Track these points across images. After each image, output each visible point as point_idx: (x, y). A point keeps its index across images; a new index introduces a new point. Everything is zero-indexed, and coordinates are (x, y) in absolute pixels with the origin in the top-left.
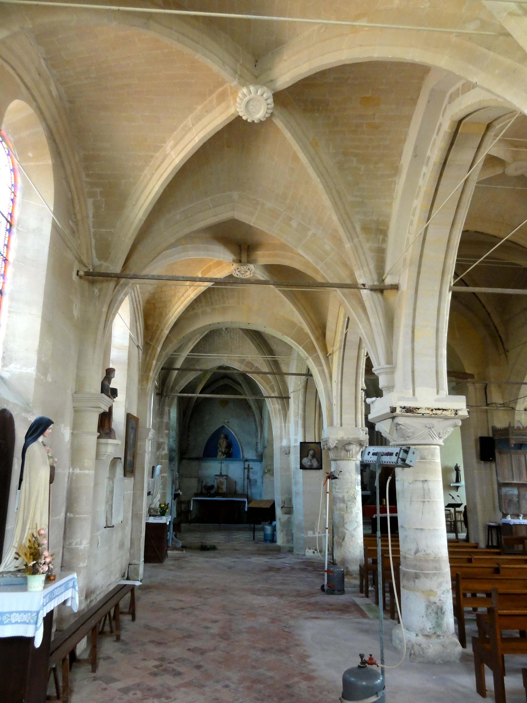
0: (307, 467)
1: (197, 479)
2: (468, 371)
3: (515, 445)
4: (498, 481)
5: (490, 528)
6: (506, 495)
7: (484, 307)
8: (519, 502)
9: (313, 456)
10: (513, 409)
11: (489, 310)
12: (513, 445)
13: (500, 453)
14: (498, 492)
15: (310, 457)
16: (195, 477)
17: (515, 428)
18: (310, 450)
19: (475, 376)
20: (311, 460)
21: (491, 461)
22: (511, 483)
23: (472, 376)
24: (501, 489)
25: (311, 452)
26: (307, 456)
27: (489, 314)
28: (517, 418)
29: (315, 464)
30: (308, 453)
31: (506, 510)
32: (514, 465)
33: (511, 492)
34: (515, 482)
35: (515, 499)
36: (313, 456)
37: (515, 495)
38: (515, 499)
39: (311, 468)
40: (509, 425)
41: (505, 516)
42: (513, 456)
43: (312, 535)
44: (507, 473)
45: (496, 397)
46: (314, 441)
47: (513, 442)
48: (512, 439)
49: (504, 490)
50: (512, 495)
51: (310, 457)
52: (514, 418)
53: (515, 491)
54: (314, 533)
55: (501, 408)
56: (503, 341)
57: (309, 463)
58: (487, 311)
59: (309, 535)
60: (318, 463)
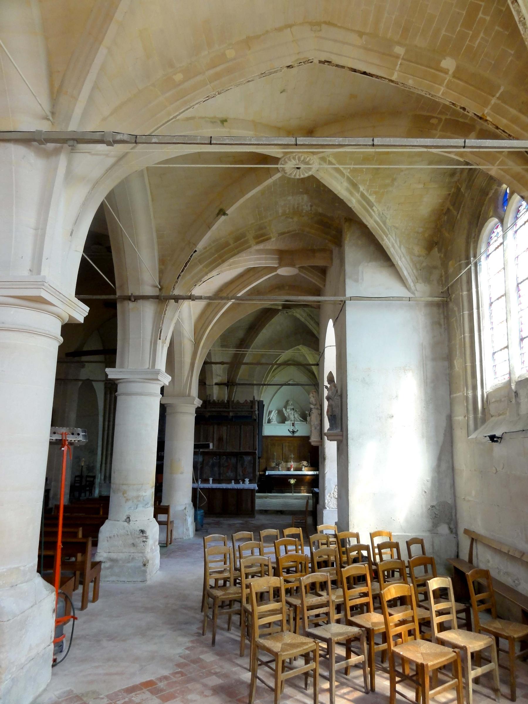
10: (205, 384)
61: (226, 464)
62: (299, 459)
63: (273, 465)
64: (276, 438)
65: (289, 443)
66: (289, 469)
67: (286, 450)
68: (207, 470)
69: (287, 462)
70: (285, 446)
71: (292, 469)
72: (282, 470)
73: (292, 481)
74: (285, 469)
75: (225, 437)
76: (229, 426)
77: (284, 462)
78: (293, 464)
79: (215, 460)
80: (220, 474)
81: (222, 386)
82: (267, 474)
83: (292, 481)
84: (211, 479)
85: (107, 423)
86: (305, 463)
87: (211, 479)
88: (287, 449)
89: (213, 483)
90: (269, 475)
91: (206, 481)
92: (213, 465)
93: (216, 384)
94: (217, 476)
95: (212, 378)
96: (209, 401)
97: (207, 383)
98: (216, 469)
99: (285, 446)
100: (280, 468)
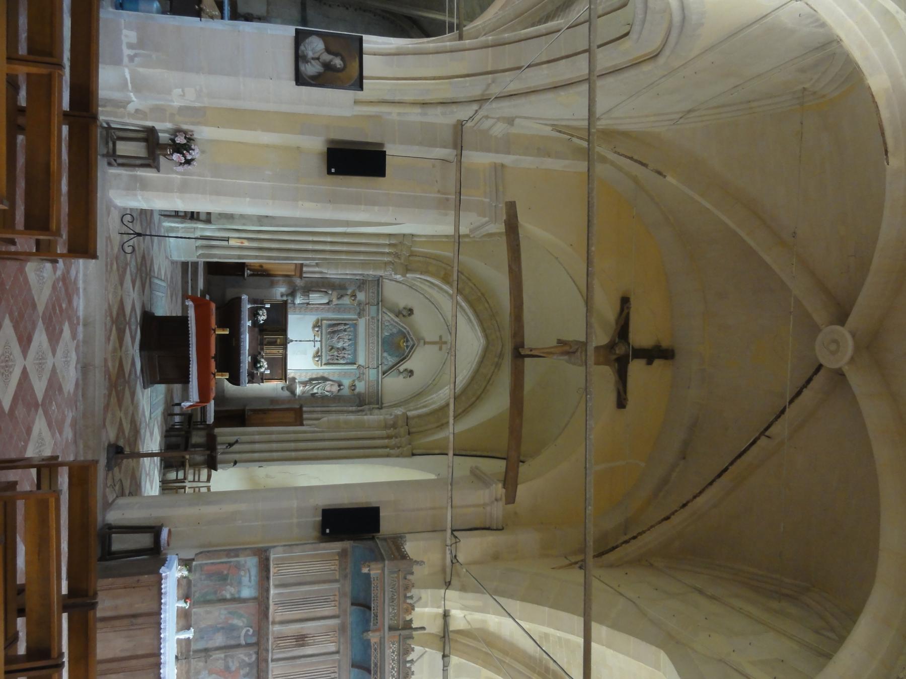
0: (302, 48)
1: (265, 14)
2: (521, 489)
3: (368, 576)
4: (274, 547)
5: (155, 530)
6: (238, 567)
7: (684, 505)
8: (224, 600)
9: (327, 66)
10: (448, 585)
11: (675, 520)
12: (365, 570)
13: (343, 554)
14: (246, 549)
15: (327, 57)
16: (268, 12)
17: (409, 577)
18: (343, 59)
19: (510, 506)
20: (318, 59)
21: (323, 532)
22: (268, 578)
23: (511, 498)
24: (255, 555)
25: (338, 62)
26: (328, 50)
27: (667, 518)
28: (427, 594)
29: (312, 69)
30: (336, 54)
31: (201, 566)
32: (316, 587)
33: (245, 580)
34: (272, 591)
35: (228, 592)
36: (327, 66)
37: (239, 592)
38: (228, 592)
39: (299, 58)
40: (417, 562)
41: (186, 563)
42: (336, 586)
43: (125, 40)
44: (293, 571)
45: (471, 547)
46: (365, 73)
47: (374, 570)
48: (383, 570)
49: (251, 562)
50: (240, 583)
51: (327, 57)
52: (426, 587)
53: (247, 592)
54: (130, 46)
55: (448, 557)
56: (605, 557)
57: (310, 54)
58: (673, 513)
59: (125, 32)
60: (314, 78)
61: (234, 666)
68: (217, 614)
75: (309, 650)
76: (337, 657)
79: (245, 633)
80: (206, 652)
81: (440, 621)
84: (189, 634)
85: (329, 239)
87: (189, 634)
89: (179, 641)
91: (185, 620)
92: (230, 629)
93: (446, 615)
94: (201, 645)
95: (465, 608)
96: (411, 637)
97: (451, 594)
98: (219, 640)
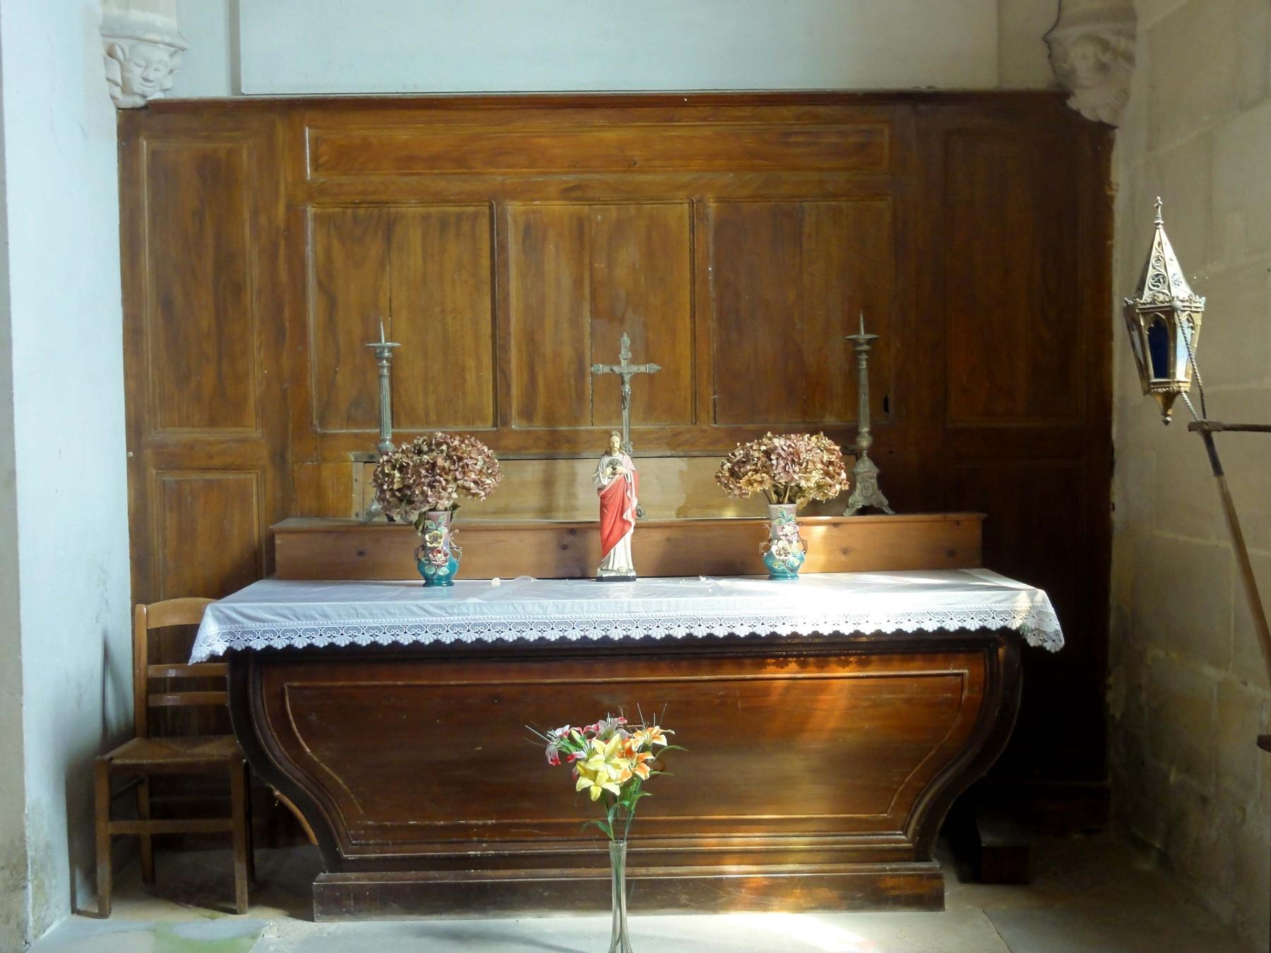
62: (739, 398)
63: (364, 500)
64: (404, 134)
65: (569, 193)
66: (574, 555)
67: (546, 286)
69: (559, 446)
70: (532, 235)
71: (621, 557)
72: (471, 568)
73: (609, 761)
74: (526, 546)
77: (507, 453)
78: (631, 476)
82: (212, 640)
83: (609, 761)
86: (813, 458)
88: (558, 266)
90: (240, 661)
99: (532, 235)
100: (441, 535)
